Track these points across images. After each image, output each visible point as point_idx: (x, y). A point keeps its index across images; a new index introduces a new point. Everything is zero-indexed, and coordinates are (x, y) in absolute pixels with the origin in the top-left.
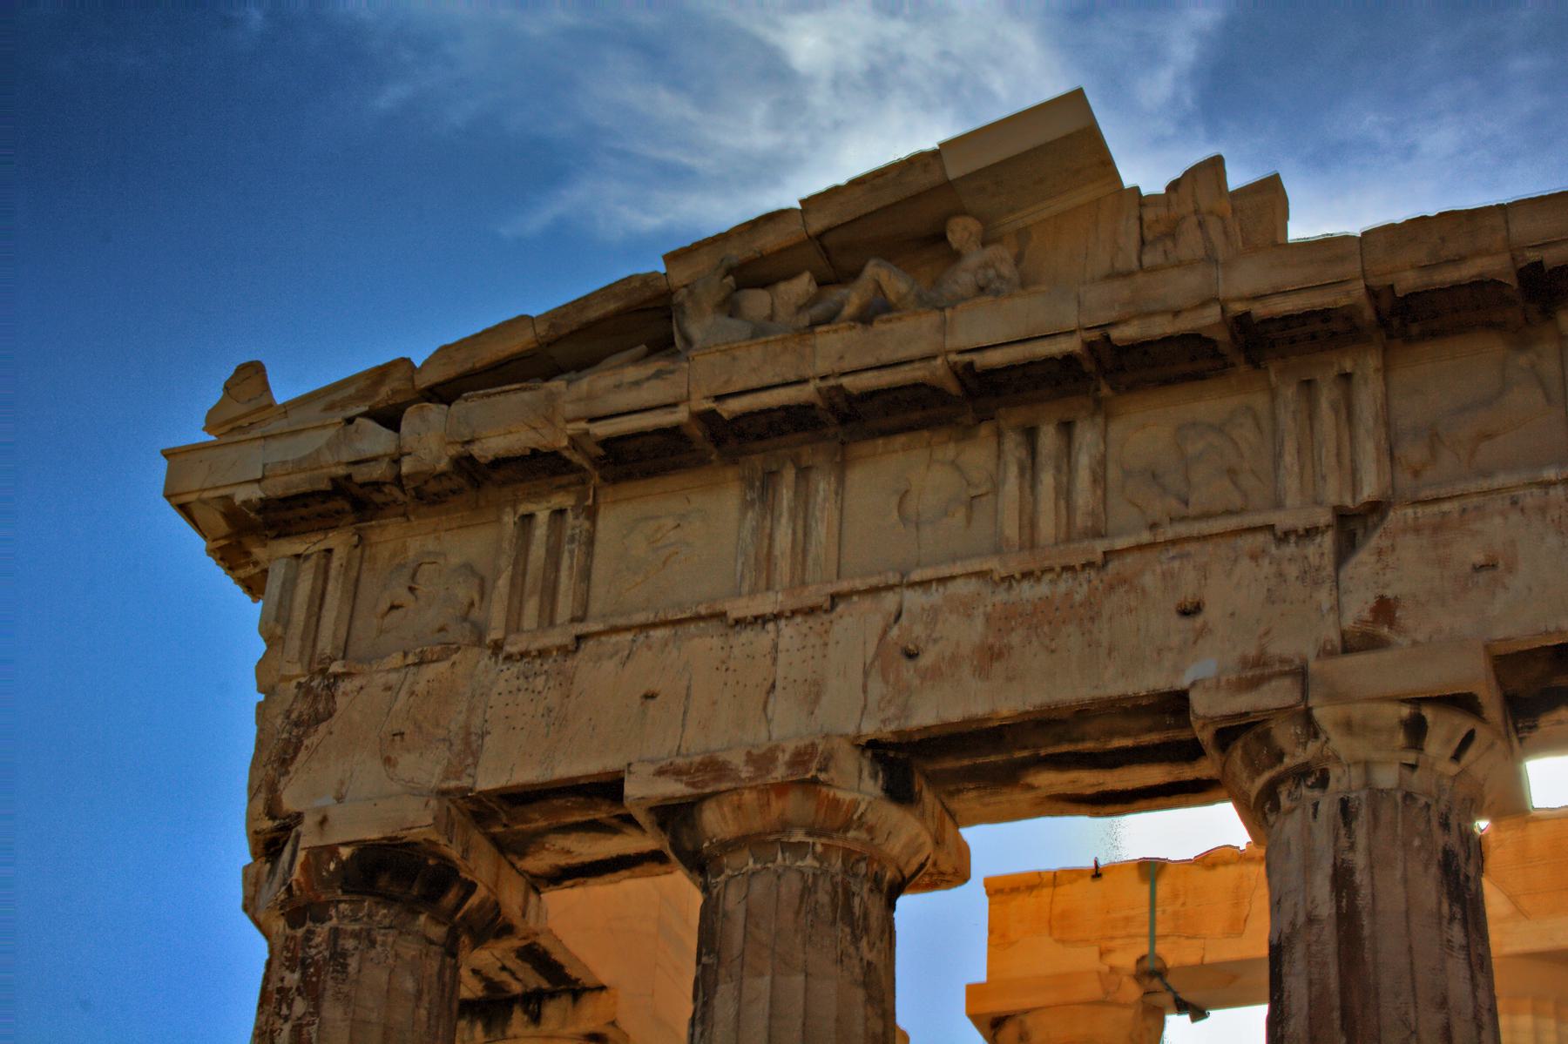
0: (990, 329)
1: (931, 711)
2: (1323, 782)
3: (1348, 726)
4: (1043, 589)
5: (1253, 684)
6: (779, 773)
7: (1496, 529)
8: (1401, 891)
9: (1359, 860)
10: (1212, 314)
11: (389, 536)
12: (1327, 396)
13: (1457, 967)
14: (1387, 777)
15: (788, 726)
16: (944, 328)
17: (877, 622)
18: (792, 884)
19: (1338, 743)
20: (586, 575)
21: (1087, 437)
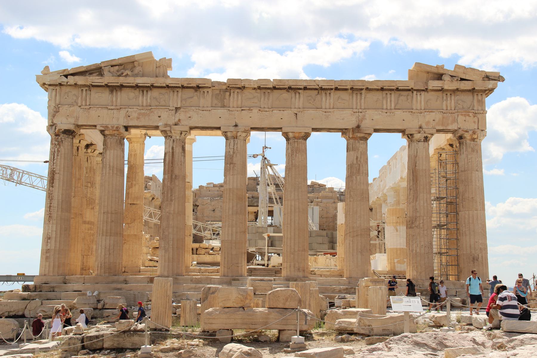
0: (140, 81)
2: (171, 137)
3: (175, 133)
5: (166, 127)
6: (115, 129)
8: (178, 150)
9: (174, 146)
10: (164, 85)
11: (63, 88)
12: (176, 93)
13: (183, 157)
14: (178, 138)
15: (115, 123)
16: (135, 80)
17: (125, 112)
18: (115, 140)
19: (173, 134)
20: (90, 99)
21: (149, 93)
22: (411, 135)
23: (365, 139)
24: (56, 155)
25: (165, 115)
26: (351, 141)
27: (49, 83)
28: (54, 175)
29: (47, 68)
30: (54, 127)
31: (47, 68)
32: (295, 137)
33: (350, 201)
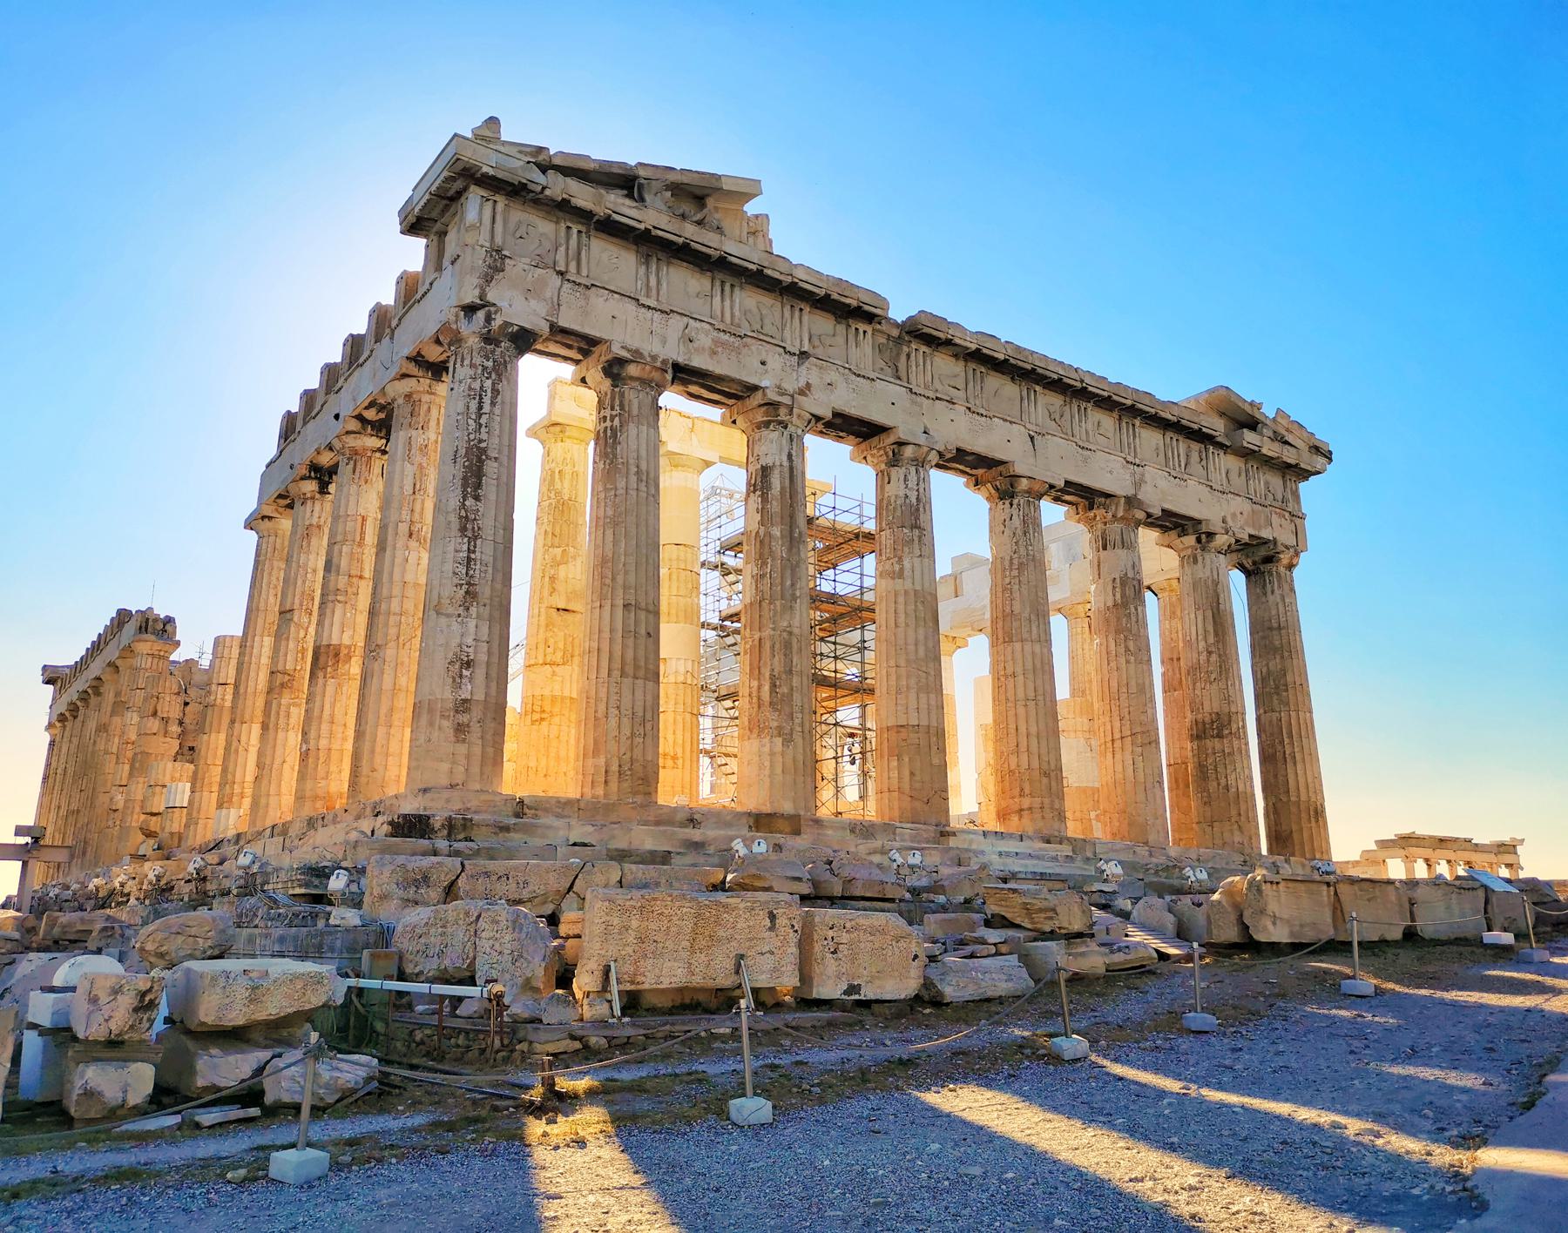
0: (733, 248)
1: (698, 362)
4: (727, 337)
5: (783, 394)
6: (658, 364)
7: (832, 376)
10: (789, 279)
12: (797, 313)
17: (682, 326)
22: (1210, 535)
23: (1138, 524)
24: (487, 400)
25: (776, 361)
26: (1117, 526)
27: (491, 172)
28: (481, 461)
29: (493, 122)
30: (481, 314)
31: (493, 122)
32: (1029, 492)
33: (1128, 662)
